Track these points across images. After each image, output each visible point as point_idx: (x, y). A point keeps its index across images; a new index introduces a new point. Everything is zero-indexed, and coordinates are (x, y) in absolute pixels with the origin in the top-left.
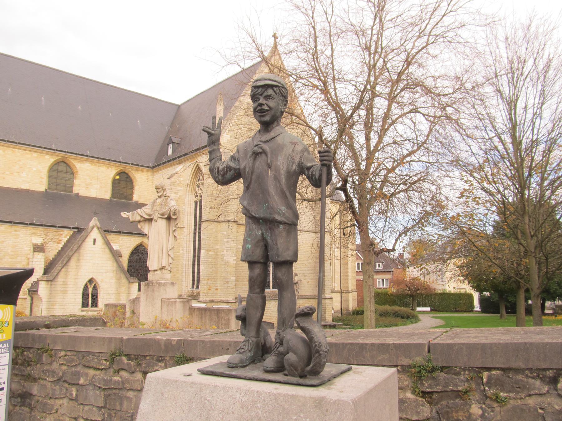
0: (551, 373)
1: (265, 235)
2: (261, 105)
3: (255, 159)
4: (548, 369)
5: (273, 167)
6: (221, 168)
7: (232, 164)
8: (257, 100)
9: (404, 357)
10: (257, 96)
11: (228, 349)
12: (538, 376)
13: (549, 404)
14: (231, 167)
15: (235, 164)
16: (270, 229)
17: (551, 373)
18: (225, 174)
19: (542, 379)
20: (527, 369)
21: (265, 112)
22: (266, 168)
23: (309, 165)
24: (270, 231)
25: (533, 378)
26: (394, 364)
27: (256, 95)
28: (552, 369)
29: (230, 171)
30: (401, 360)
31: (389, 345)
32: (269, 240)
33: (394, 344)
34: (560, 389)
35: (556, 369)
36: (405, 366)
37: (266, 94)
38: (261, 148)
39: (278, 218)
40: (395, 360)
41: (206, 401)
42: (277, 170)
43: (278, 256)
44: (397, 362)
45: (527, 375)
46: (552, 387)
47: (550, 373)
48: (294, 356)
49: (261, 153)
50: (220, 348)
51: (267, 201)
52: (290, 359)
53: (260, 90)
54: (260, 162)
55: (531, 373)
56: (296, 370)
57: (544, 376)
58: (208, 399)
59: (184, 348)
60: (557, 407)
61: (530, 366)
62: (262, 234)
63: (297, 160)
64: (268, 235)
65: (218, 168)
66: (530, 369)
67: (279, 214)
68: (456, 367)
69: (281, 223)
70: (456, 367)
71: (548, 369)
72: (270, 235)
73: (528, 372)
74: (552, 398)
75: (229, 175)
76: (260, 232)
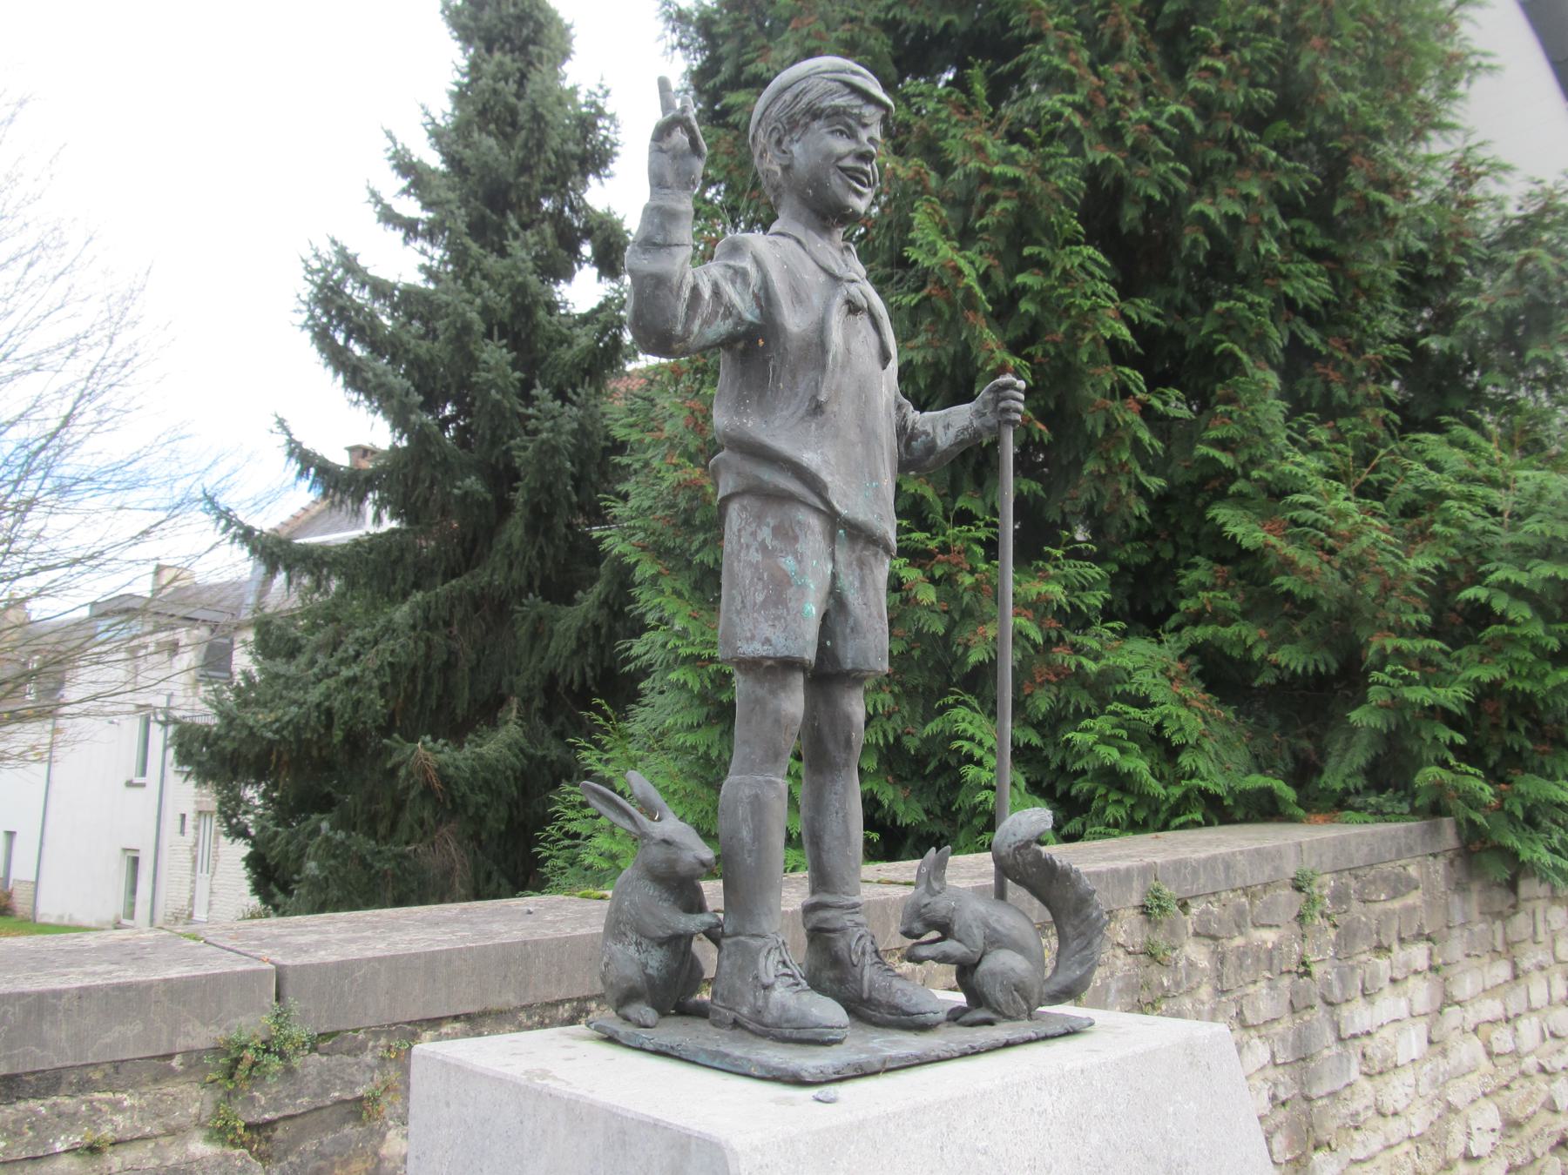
4: (561, 1002)
8: (842, 133)
9: (198, 1023)
10: (852, 122)
14: (733, 306)
15: (743, 300)
20: (523, 1008)
21: (863, 184)
24: (857, 571)
26: (161, 1053)
27: (850, 115)
28: (570, 1000)
29: (725, 317)
30: (188, 1034)
31: (149, 986)
33: (166, 981)
36: (200, 1051)
40: (164, 1037)
41: (980, 1157)
44: (171, 1042)
45: (521, 1023)
48: (1019, 957)
52: (1013, 969)
55: (529, 1017)
58: (981, 1145)
64: (852, 584)
66: (527, 1008)
68: (356, 1031)
70: (356, 1031)
71: (561, 1002)
72: (857, 584)
73: (522, 1016)
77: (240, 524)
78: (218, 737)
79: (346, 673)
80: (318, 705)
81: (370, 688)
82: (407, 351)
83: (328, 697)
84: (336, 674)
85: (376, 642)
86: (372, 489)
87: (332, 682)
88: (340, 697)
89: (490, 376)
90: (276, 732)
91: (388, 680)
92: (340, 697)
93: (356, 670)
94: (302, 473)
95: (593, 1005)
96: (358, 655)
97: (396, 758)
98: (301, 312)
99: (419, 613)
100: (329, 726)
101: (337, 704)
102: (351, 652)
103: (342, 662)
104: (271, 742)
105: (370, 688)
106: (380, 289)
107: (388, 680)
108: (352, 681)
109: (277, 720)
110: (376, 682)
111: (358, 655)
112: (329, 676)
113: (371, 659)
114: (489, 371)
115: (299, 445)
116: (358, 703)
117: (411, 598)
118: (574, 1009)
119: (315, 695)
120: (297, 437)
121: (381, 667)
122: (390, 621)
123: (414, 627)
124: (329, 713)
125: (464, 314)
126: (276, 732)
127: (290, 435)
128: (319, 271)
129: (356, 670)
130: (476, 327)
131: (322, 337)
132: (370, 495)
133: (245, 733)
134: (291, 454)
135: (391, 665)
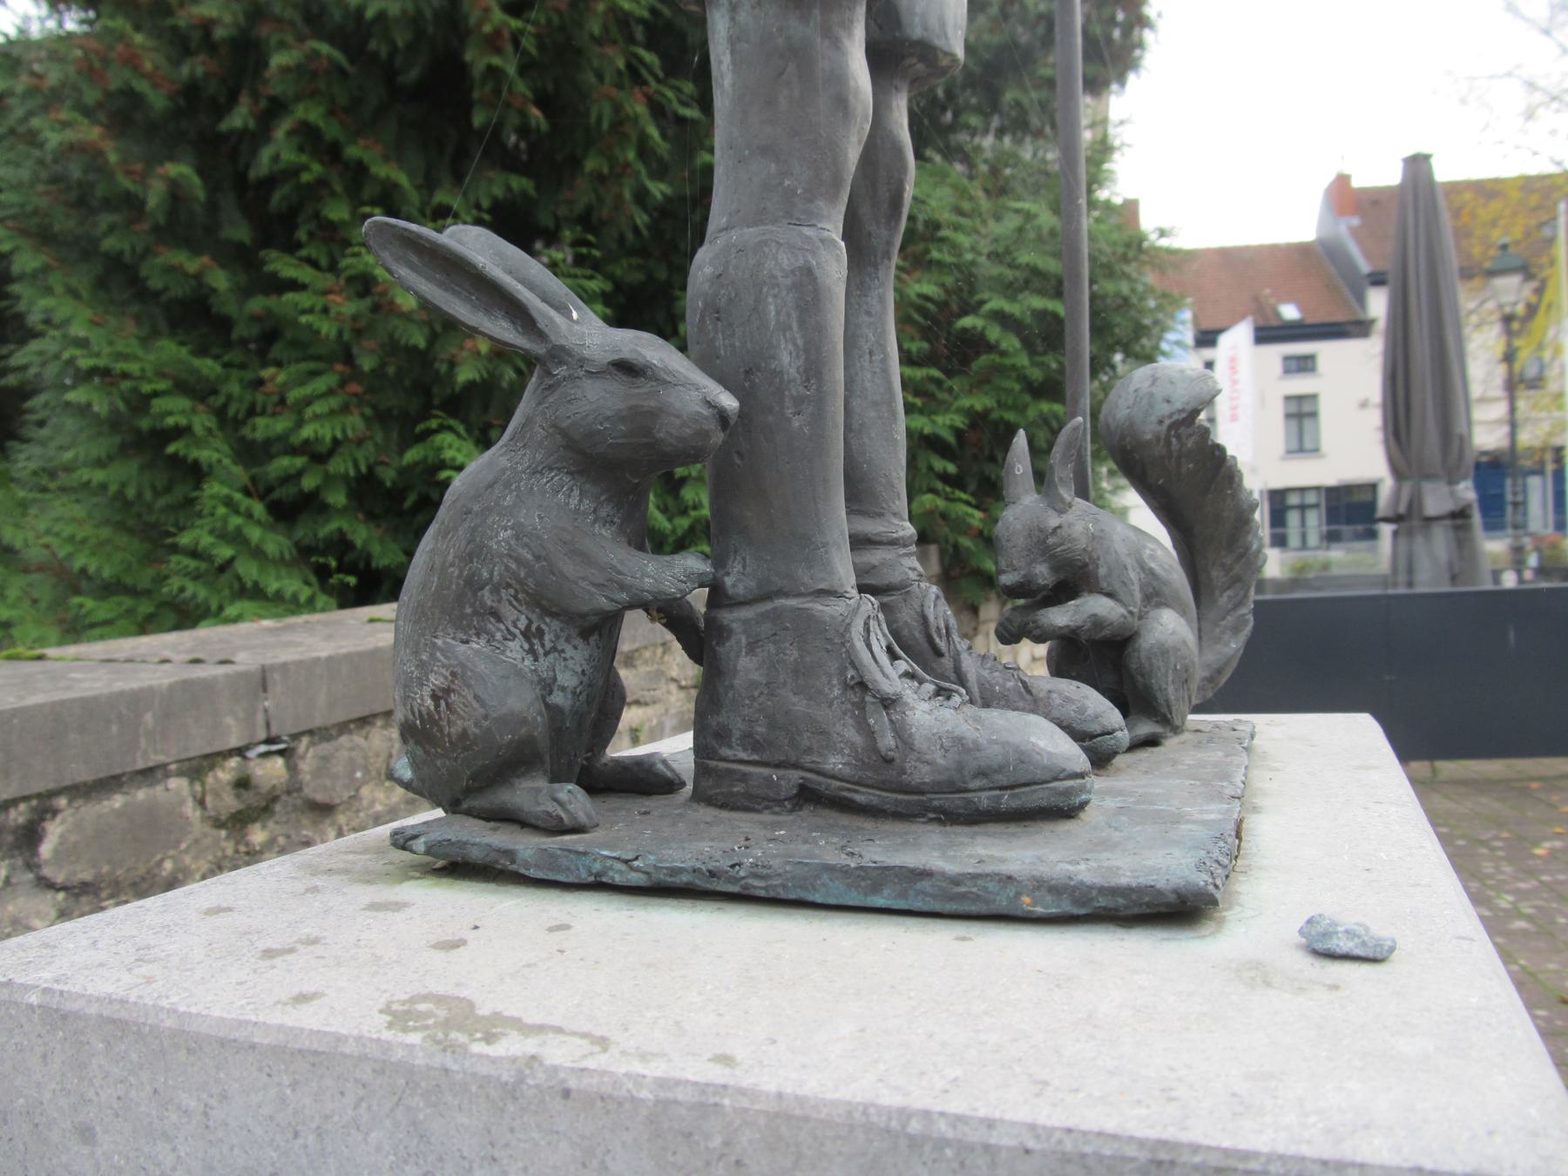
0: (21, 814)
4: (14, 802)
17: (21, 814)
28: (26, 799)
34: (47, 861)
35: (39, 796)
46: (19, 862)
71: (14, 802)
74: (21, 901)
95: (62, 802)
118: (33, 810)
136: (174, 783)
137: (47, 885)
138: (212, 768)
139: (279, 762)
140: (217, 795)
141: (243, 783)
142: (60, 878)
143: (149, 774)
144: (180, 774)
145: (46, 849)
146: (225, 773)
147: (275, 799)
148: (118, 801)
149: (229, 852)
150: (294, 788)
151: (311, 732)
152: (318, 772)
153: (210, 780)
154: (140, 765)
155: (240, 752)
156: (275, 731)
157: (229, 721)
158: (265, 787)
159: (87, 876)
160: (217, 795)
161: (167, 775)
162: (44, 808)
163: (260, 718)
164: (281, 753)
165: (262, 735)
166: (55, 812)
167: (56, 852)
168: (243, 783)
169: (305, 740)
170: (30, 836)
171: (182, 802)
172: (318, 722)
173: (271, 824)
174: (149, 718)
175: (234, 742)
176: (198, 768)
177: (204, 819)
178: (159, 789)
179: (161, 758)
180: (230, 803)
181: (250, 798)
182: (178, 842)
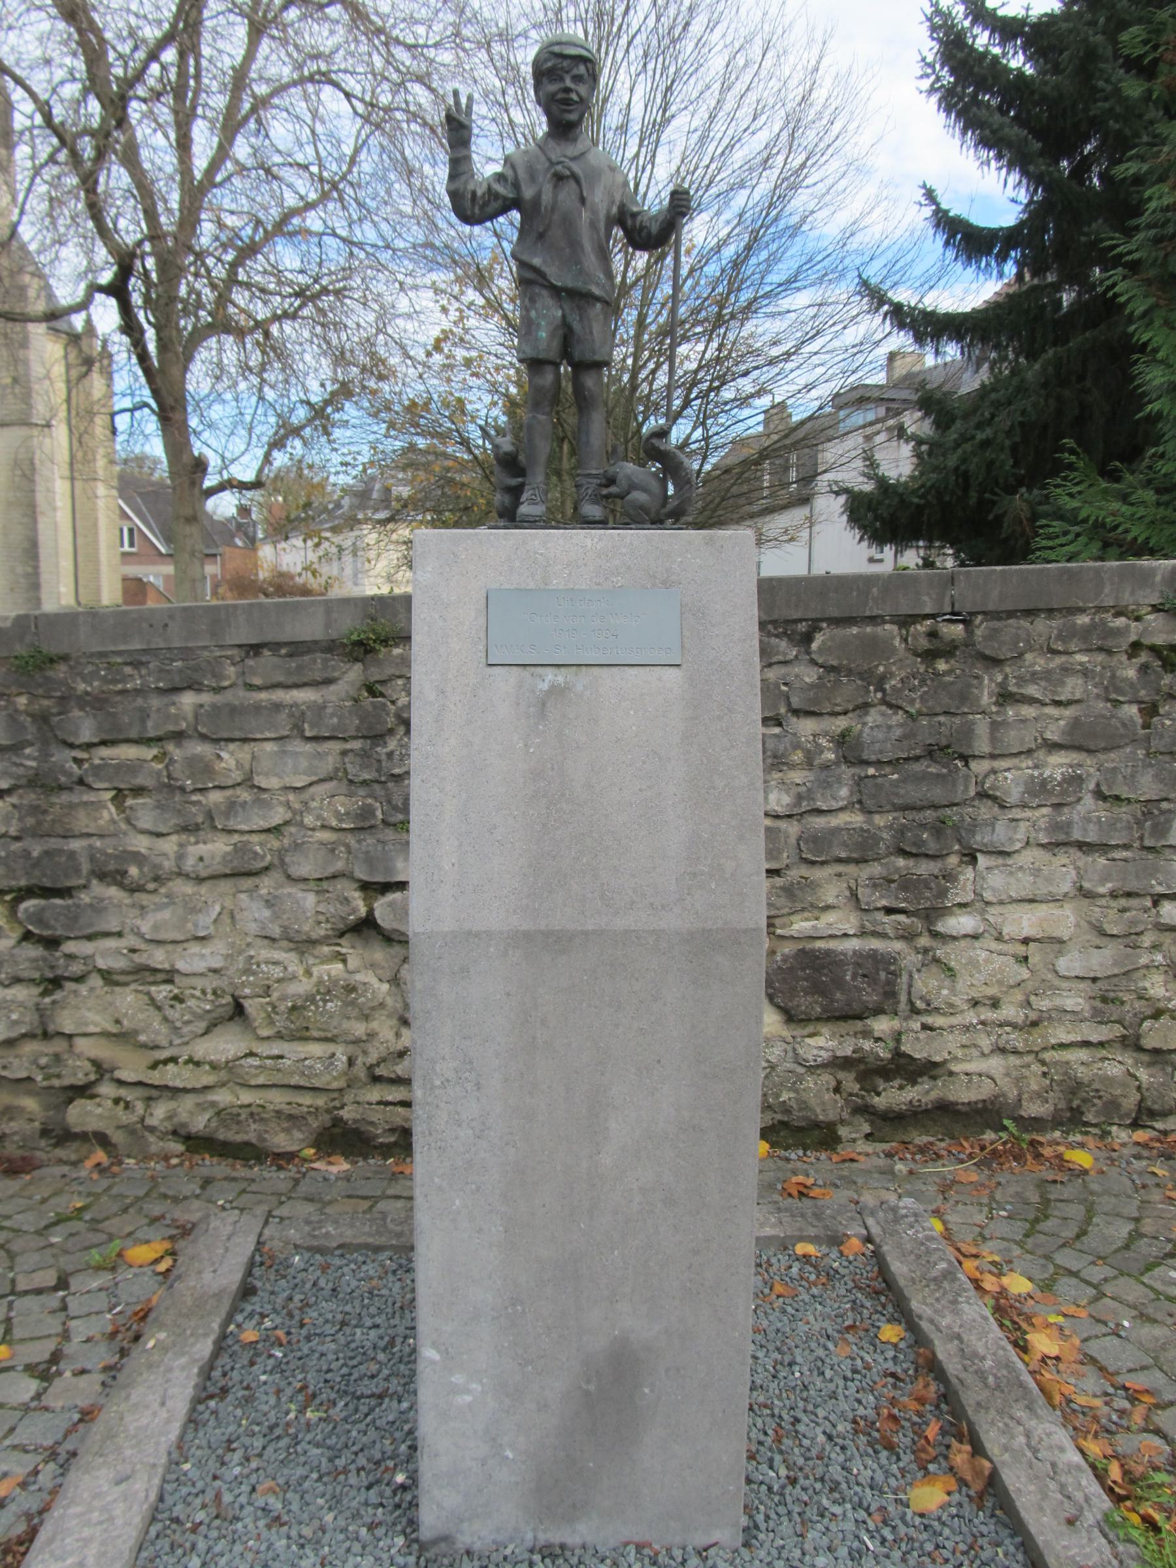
1: (569, 319)
2: (568, 90)
3: (555, 187)
4: (801, 620)
5: (588, 203)
6: (479, 192)
7: (499, 188)
11: (166, 625)
12: (785, 633)
13: (797, 676)
16: (579, 308)
18: (485, 204)
19: (790, 638)
22: (578, 205)
23: (635, 209)
25: (777, 636)
32: (576, 326)
37: (575, 72)
38: (569, 169)
39: (596, 291)
42: (594, 212)
43: (594, 352)
47: (802, 627)
49: (567, 177)
50: (145, 625)
51: (578, 262)
53: (565, 63)
54: (567, 194)
56: (647, 514)
57: (794, 632)
59: (36, 634)
60: (807, 680)
61: (775, 617)
62: (564, 316)
63: (618, 198)
65: (474, 193)
67: (597, 284)
69: (598, 299)
71: (801, 620)
75: (495, 205)
76: (560, 313)
77: (890, 302)
78: (879, 503)
79: (980, 436)
80: (957, 469)
81: (1002, 449)
82: (1032, 92)
83: (964, 460)
84: (973, 438)
85: (1010, 403)
86: (1015, 248)
87: (968, 447)
88: (975, 460)
89: (1107, 105)
90: (922, 497)
91: (1017, 439)
92: (975, 460)
93: (988, 432)
94: (947, 244)
95: (824, 625)
96: (993, 416)
97: (997, 510)
98: (927, 76)
99: (1050, 369)
100: (966, 488)
101: (972, 467)
102: (987, 414)
103: (979, 426)
104: (918, 506)
105: (1002, 449)
106: (1007, 29)
107: (1017, 439)
108: (986, 444)
109: (922, 486)
110: (1007, 443)
111: (993, 416)
112: (967, 440)
113: (1004, 420)
114: (1106, 99)
115: (946, 212)
116: (990, 464)
117: (1044, 357)
119: (952, 461)
120: (944, 206)
121: (1012, 427)
122: (1022, 381)
123: (1045, 385)
124: (966, 476)
125: (1085, 40)
126: (922, 497)
127: (938, 205)
128: (940, 27)
129: (988, 432)
130: (1100, 51)
131: (950, 101)
132: (1013, 254)
133: (896, 500)
134: (937, 226)
135: (1022, 424)
136: (887, 627)
137: (814, 662)
138: (914, 623)
139: (961, 627)
140: (915, 638)
141: (933, 634)
142: (820, 661)
143: (874, 620)
144: (891, 622)
145: (814, 646)
146: (922, 628)
147: (956, 648)
148: (855, 630)
149: (922, 669)
150: (968, 643)
151: (984, 613)
152: (986, 638)
153: (912, 629)
154: (868, 613)
155: (933, 616)
156: (956, 609)
157: (926, 598)
158: (948, 638)
159: (835, 663)
160: (915, 638)
161: (885, 622)
162: (815, 627)
163: (947, 600)
164: (962, 621)
165: (949, 610)
166: (821, 629)
167: (819, 648)
168: (933, 634)
169: (980, 617)
170: (808, 638)
171: (893, 638)
172: (991, 607)
173: (952, 661)
174: (875, 590)
175: (928, 610)
176: (905, 621)
177: (908, 649)
178: (879, 629)
179: (880, 612)
180: (924, 643)
181: (936, 644)
182: (888, 659)
